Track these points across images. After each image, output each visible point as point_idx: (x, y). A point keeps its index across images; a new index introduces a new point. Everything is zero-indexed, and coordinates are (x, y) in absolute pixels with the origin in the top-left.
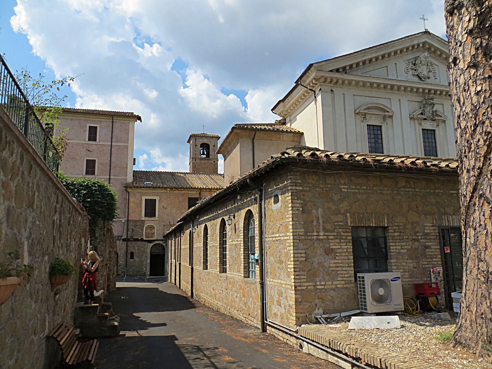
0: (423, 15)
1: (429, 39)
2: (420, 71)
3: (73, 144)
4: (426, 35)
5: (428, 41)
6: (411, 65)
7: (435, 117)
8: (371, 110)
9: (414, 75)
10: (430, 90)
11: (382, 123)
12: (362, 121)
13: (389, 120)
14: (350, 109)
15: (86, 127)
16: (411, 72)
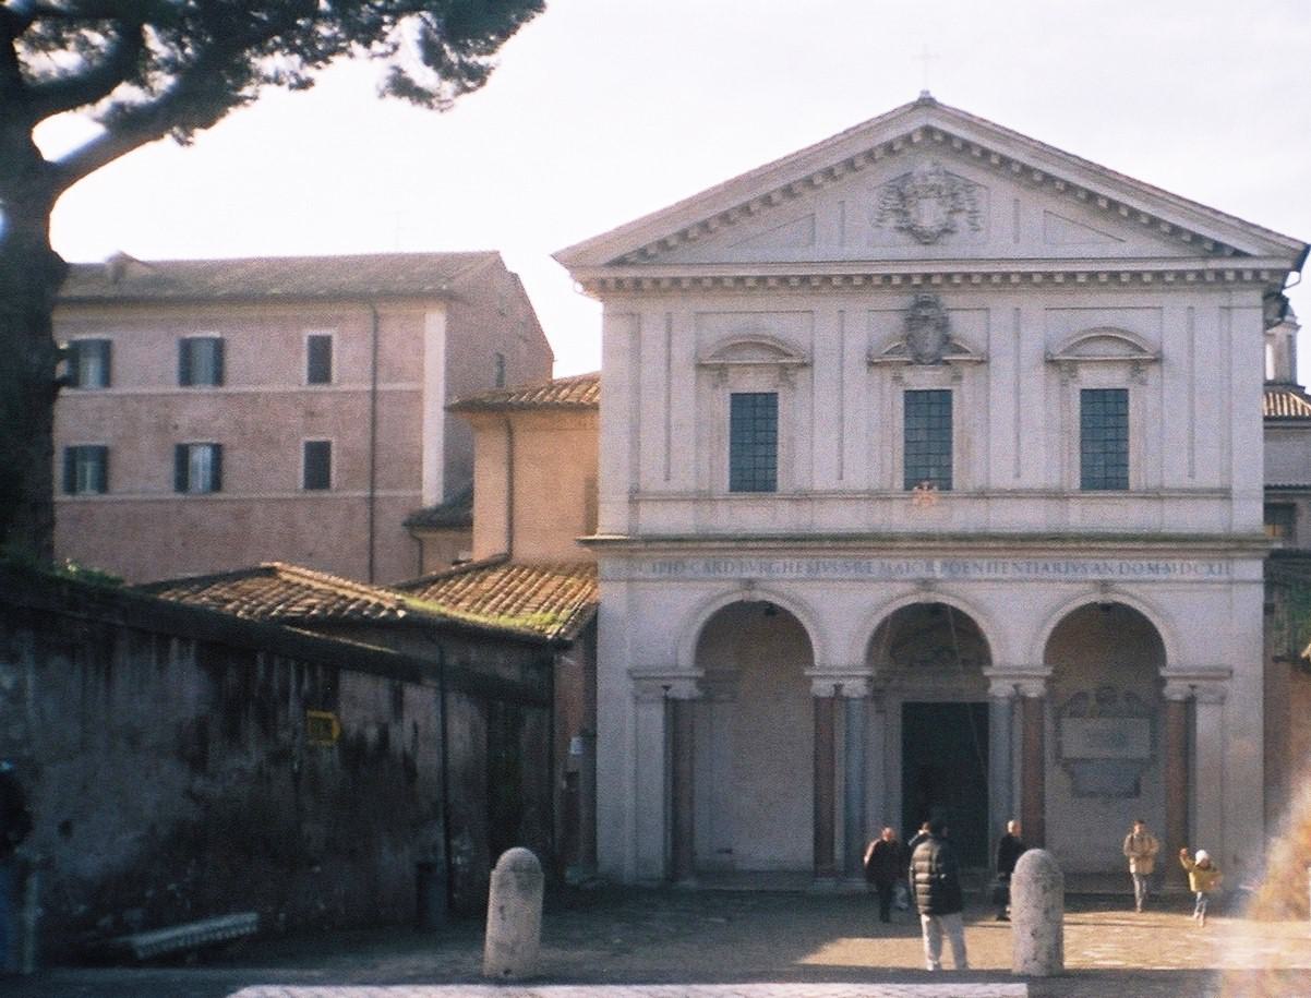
2: (913, 216)
3: (266, 395)
6: (894, 200)
7: (946, 355)
8: (746, 354)
9: (901, 229)
10: (927, 277)
11: (777, 386)
14: (683, 352)
15: (300, 338)
16: (892, 222)
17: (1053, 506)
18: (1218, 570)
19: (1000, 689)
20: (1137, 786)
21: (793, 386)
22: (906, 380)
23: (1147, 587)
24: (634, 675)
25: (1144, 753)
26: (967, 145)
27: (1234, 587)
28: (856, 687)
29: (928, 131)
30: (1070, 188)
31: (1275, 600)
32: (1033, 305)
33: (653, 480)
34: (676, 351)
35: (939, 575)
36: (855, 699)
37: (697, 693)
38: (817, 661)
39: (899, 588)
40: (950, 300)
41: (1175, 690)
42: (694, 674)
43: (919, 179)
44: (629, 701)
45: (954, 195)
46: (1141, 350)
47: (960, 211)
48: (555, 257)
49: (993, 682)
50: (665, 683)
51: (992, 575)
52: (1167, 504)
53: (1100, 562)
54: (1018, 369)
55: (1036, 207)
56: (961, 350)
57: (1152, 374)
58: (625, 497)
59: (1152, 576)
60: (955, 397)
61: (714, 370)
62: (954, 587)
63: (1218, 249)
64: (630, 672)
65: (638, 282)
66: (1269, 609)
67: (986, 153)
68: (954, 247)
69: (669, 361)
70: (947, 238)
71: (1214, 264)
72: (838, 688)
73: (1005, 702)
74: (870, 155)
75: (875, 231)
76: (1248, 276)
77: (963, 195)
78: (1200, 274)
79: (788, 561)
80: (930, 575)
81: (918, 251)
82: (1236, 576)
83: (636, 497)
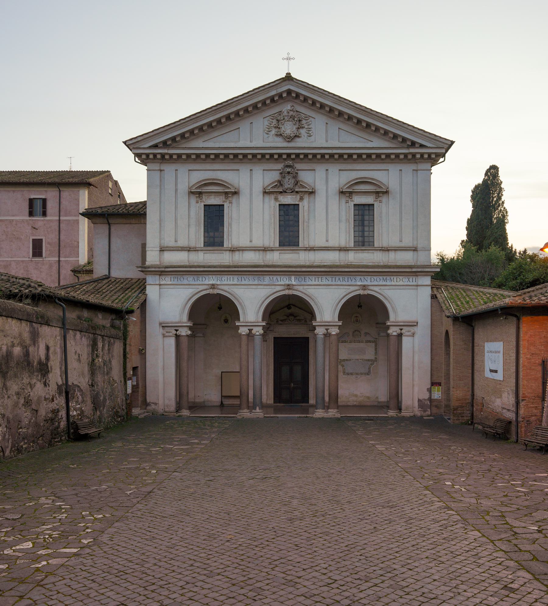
0: (288, 54)
1: (292, 85)
2: (283, 129)
4: (287, 82)
5: (292, 88)
6: (275, 122)
9: (277, 135)
10: (289, 155)
11: (224, 202)
12: (197, 202)
13: (234, 199)
16: (274, 131)
17: (342, 254)
18: (412, 281)
19: (320, 331)
20: (369, 368)
21: (231, 203)
22: (279, 199)
23: (382, 288)
24: (163, 326)
25: (373, 357)
26: (306, 99)
27: (419, 287)
28: (258, 331)
29: (289, 92)
30: (350, 118)
31: (436, 293)
32: (334, 169)
33: (169, 241)
34: (180, 186)
35: (294, 283)
36: (257, 335)
37: (189, 332)
38: (241, 319)
39: (278, 288)
40: (298, 166)
41: (393, 331)
42: (189, 324)
43: (285, 112)
44: (161, 336)
45: (300, 121)
46: (380, 187)
47: (303, 128)
48: (125, 143)
49: (317, 328)
50: (177, 328)
51: (317, 283)
52: (390, 252)
53: (362, 278)
54: (327, 197)
55: (335, 126)
56: (303, 187)
57: (384, 199)
58: (159, 249)
59: (384, 283)
60: (300, 206)
61: (196, 194)
62: (301, 288)
63: (413, 144)
64: (160, 324)
65: (163, 156)
66: (434, 297)
67: (314, 102)
68: (299, 143)
69: (176, 190)
70: (297, 139)
71: (412, 150)
72: (250, 330)
73: (322, 336)
74: (264, 102)
75: (267, 136)
76: (426, 156)
77: (304, 122)
78: (406, 155)
79: (229, 277)
80: (290, 283)
81: (285, 144)
82: (420, 283)
83: (162, 250)
